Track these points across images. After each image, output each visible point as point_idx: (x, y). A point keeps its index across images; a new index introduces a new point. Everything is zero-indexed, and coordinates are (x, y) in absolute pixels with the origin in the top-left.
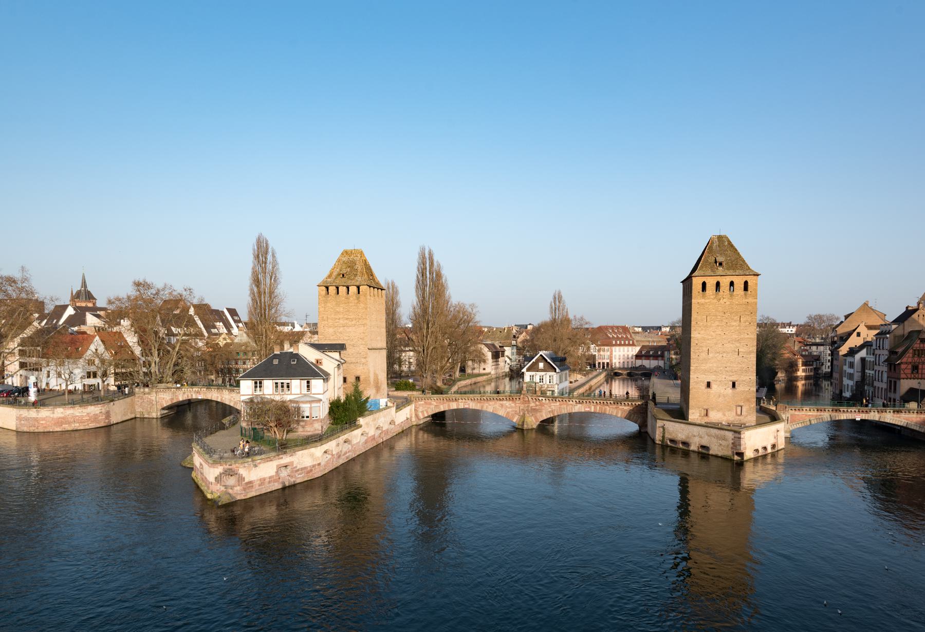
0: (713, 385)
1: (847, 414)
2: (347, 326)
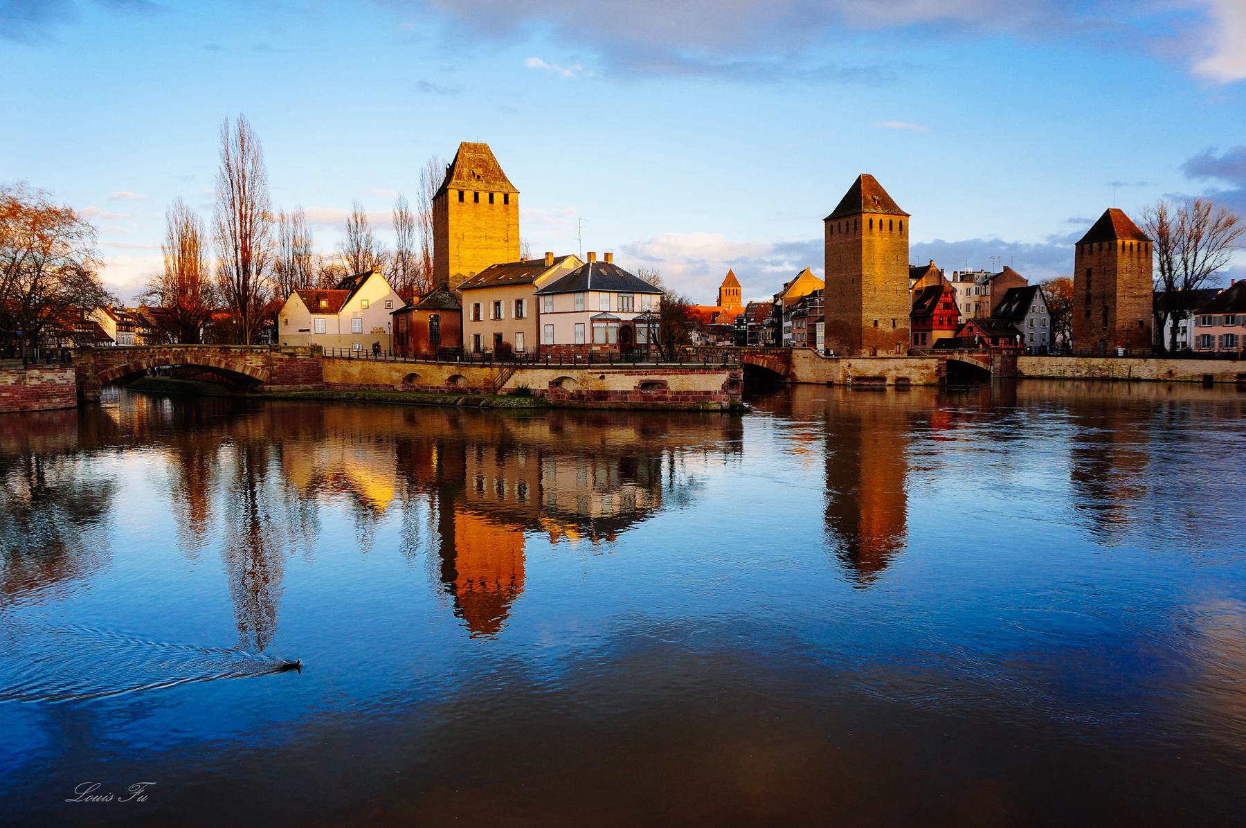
0: (880, 325)
2: (492, 249)
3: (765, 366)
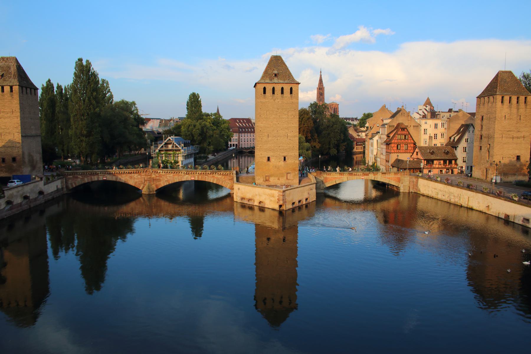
0: (272, 159)
1: (357, 176)
3: (215, 182)
